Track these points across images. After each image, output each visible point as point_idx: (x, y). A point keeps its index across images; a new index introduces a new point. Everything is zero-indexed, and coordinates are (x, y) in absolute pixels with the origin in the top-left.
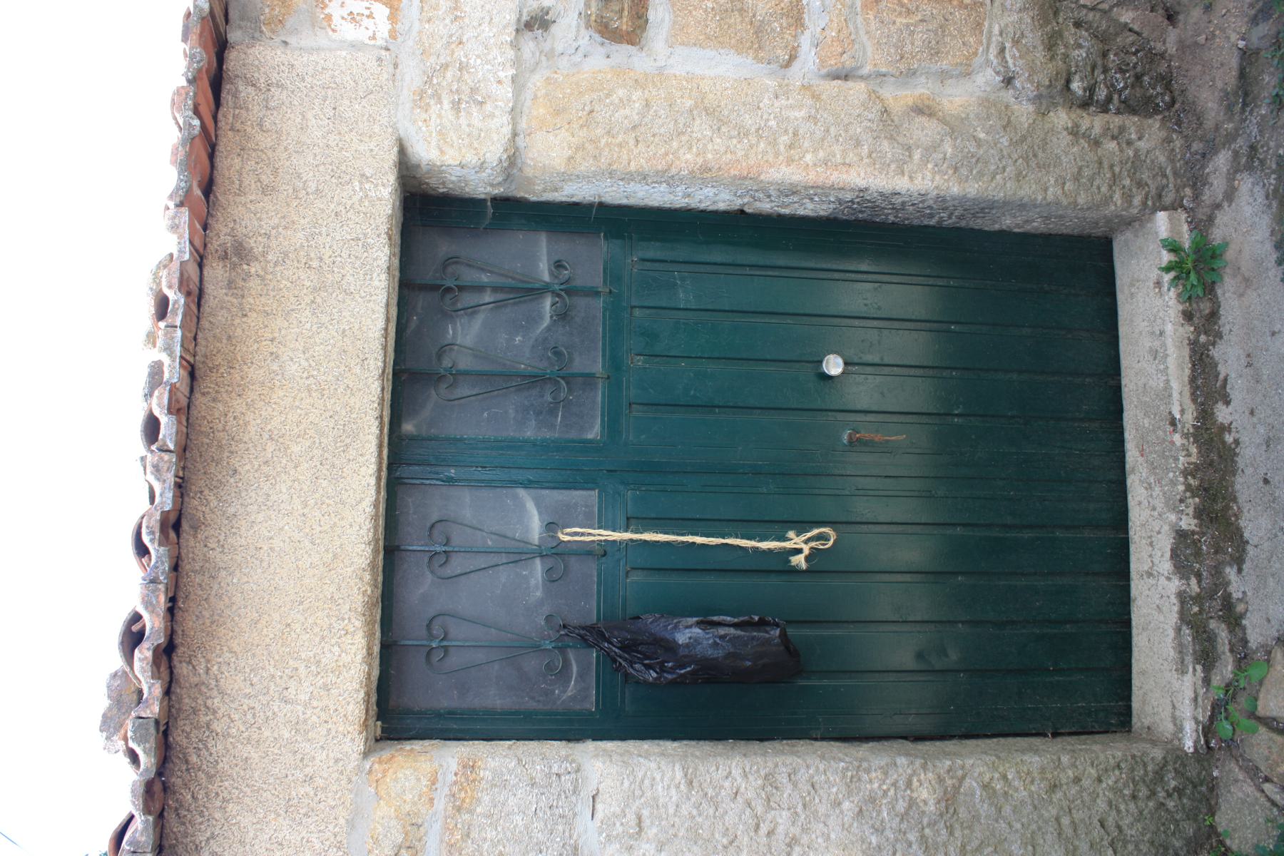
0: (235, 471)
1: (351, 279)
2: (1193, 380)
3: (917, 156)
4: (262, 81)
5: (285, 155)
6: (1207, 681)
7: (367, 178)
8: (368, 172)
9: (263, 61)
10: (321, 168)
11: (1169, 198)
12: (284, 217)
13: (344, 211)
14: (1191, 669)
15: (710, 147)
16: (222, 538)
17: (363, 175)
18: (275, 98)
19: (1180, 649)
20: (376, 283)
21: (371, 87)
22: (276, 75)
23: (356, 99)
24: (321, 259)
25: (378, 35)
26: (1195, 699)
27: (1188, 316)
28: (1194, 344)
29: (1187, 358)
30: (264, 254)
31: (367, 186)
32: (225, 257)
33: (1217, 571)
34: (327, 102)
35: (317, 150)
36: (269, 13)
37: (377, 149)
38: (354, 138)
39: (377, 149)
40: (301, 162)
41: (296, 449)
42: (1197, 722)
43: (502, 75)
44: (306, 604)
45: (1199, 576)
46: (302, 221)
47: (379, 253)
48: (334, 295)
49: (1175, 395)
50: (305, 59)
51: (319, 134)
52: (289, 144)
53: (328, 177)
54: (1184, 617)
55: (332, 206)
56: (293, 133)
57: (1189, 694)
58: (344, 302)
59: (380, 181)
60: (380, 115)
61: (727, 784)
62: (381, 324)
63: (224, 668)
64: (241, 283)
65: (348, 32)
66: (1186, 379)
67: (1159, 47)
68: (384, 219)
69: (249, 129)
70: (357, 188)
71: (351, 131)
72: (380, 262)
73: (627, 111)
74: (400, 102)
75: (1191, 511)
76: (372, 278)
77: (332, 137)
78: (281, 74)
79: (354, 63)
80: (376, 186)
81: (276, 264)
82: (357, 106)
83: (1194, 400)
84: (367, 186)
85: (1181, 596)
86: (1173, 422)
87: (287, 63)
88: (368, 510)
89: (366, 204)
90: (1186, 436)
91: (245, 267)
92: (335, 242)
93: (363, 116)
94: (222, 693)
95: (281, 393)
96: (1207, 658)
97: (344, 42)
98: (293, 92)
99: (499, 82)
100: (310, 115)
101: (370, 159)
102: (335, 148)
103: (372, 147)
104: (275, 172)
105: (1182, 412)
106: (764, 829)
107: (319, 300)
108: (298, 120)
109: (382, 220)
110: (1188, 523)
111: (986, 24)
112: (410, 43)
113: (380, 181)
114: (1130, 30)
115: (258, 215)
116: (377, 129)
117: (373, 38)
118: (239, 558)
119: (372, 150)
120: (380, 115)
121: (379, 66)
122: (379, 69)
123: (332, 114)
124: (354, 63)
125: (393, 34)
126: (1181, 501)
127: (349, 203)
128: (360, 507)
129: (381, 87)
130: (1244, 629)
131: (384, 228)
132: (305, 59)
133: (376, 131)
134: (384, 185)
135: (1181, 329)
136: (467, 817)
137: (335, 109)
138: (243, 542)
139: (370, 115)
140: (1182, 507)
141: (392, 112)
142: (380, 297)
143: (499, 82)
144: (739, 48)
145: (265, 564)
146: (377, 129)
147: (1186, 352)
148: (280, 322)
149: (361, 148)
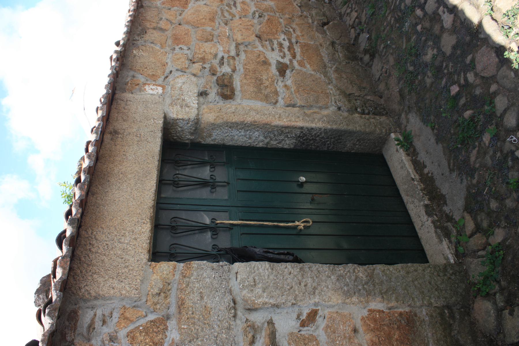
0: (109, 181)
2: (415, 169)
3: (316, 120)
6: (450, 242)
8: (156, 118)
11: (393, 130)
14: (444, 240)
15: (256, 117)
16: (102, 197)
19: (439, 237)
26: (449, 247)
27: (408, 155)
28: (412, 161)
29: (411, 164)
32: (111, 133)
33: (441, 211)
35: (140, 113)
41: (130, 176)
42: (452, 254)
43: (194, 102)
44: (130, 215)
45: (436, 215)
49: (411, 173)
54: (436, 227)
57: (446, 247)
61: (286, 270)
62: (159, 149)
63: (98, 233)
65: (151, 92)
66: (413, 169)
67: (380, 103)
73: (231, 109)
75: (427, 199)
81: (127, 135)
83: (417, 173)
85: (433, 222)
86: (413, 179)
88: (153, 191)
90: (418, 181)
94: (97, 239)
95: (126, 163)
96: (447, 234)
99: (194, 103)
104: (128, 117)
105: (415, 176)
106: (303, 284)
110: (427, 202)
111: (330, 97)
112: (168, 94)
114: (371, 100)
117: (158, 93)
118: (107, 203)
125: (163, 93)
126: (423, 197)
127: (150, 124)
128: (150, 191)
130: (454, 219)
131: (160, 129)
135: (407, 158)
136: (188, 279)
138: (109, 198)
140: (424, 198)
143: (194, 103)
144: (261, 100)
145: (117, 204)
146: (158, 110)
147: (410, 162)
148: (127, 147)
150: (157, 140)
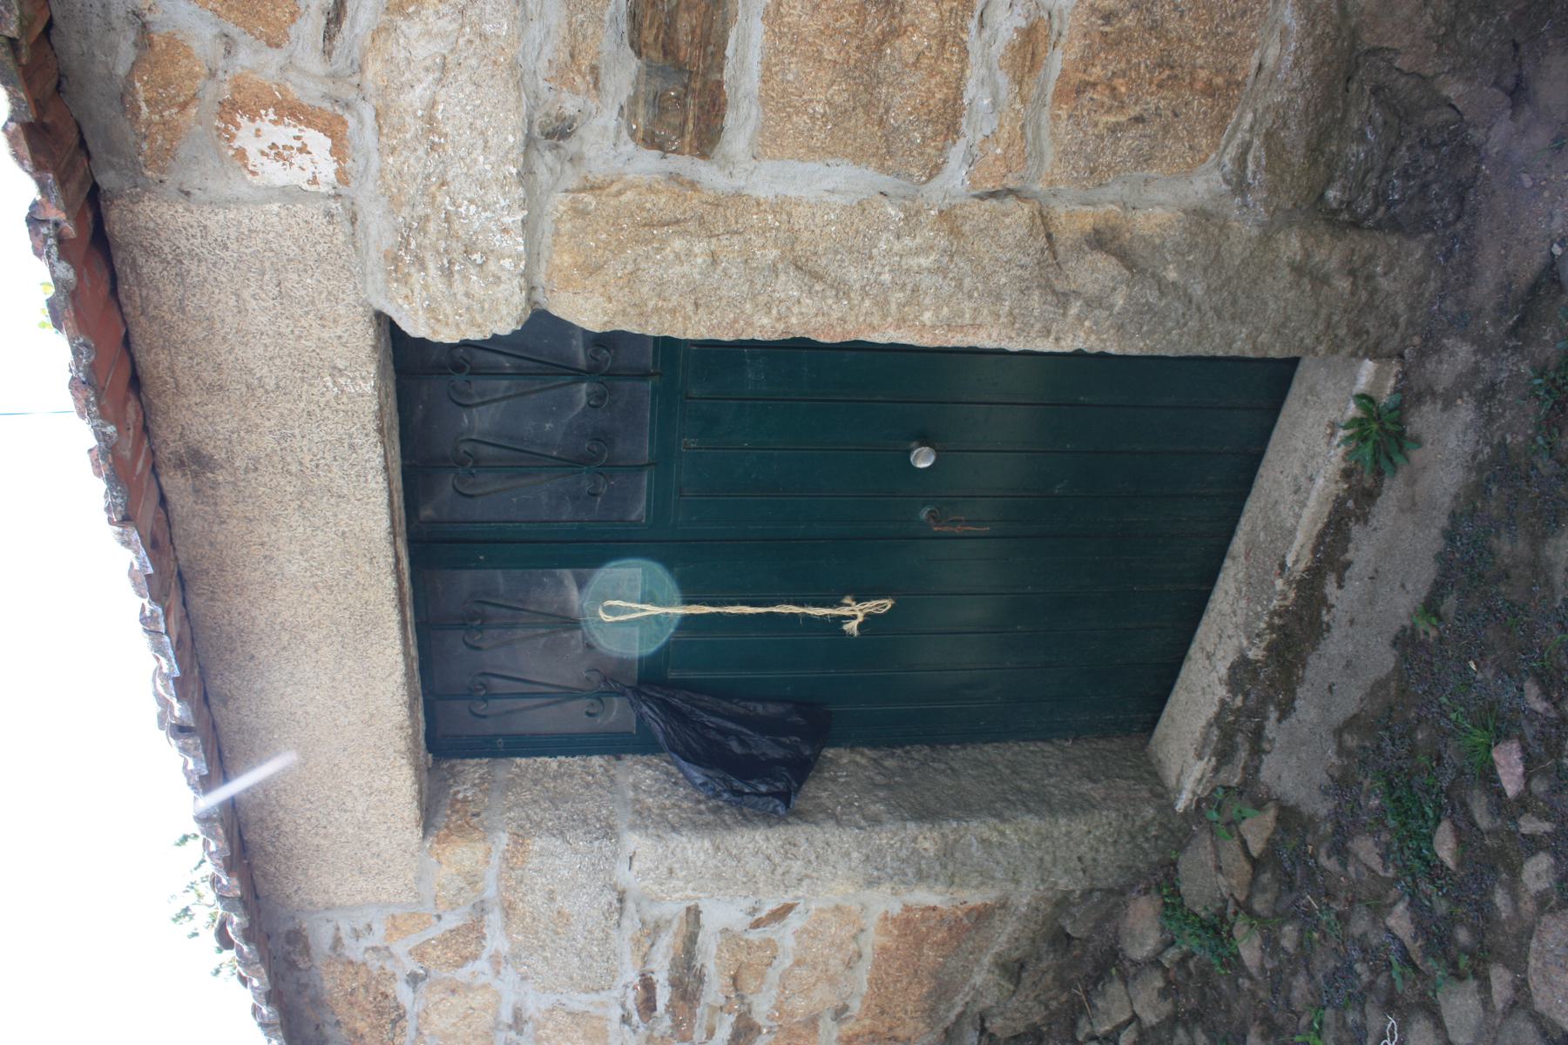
0: (252, 657)
1: (342, 481)
2: (1321, 535)
3: (1074, 310)
4: (167, 250)
5: (226, 347)
6: (1216, 770)
7: (340, 370)
8: (341, 364)
9: (159, 221)
10: (278, 361)
11: (1392, 344)
12: (242, 420)
13: (318, 410)
14: (1206, 759)
15: (796, 310)
16: (254, 708)
17: (335, 368)
18: (192, 273)
19: (1205, 738)
20: (373, 485)
21: (324, 254)
22: (184, 241)
23: (306, 271)
24: (301, 464)
25: (320, 178)
26: (1201, 780)
27: (1347, 474)
28: (1339, 503)
29: (1326, 514)
30: (230, 459)
31: (342, 381)
32: (181, 464)
33: (1263, 702)
34: (267, 277)
36: (150, 148)
37: (346, 335)
39: (346, 335)
40: (250, 355)
41: (312, 637)
42: (1194, 793)
43: (507, 220)
44: (350, 750)
45: (1246, 695)
46: (267, 424)
47: (371, 454)
48: (325, 499)
49: (1296, 545)
50: (221, 217)
51: (265, 319)
52: (227, 333)
54: (1218, 719)
55: (302, 405)
56: (228, 320)
57: (1197, 775)
58: (338, 505)
59: (357, 374)
61: (750, 846)
62: (385, 524)
63: (282, 793)
64: (210, 492)
65: (275, 174)
66: (1315, 533)
67: (1477, 135)
68: (371, 417)
69: (168, 316)
70: (330, 384)
71: (307, 313)
72: (373, 464)
73: (686, 268)
74: (369, 270)
75: (1263, 645)
76: (366, 481)
77: (283, 322)
78: (192, 240)
79: (292, 222)
80: (353, 379)
81: (246, 471)
82: (309, 281)
83: (1315, 550)
84: (342, 381)
85: (1223, 702)
86: (1283, 566)
87: (195, 224)
88: (399, 680)
89: (345, 399)
90: (1288, 583)
91: (210, 475)
92: (313, 445)
93: (321, 293)
94: (282, 807)
95: (285, 591)
96: (1224, 756)
97: (272, 188)
98: (214, 265)
99: (505, 231)
100: (246, 294)
101: (340, 349)
103: (339, 333)
104: (218, 368)
105: (1296, 562)
106: (780, 871)
107: (308, 505)
108: (232, 302)
110: (1255, 654)
111: (1235, 115)
112: (370, 186)
113: (357, 374)
114: (1453, 107)
115: (210, 419)
116: (341, 310)
117: (314, 181)
118: (275, 721)
119: (340, 337)
121: (329, 223)
122: (331, 228)
123: (276, 293)
124: (292, 222)
125: (342, 176)
126: (1258, 635)
127: (323, 401)
128: (390, 679)
130: (1261, 761)
131: (372, 426)
132: (221, 217)
134: (363, 378)
135: (1333, 487)
136: (520, 872)
138: (276, 709)
139: (329, 293)
140: (1256, 641)
141: (359, 286)
142: (380, 499)
143: (505, 231)
144: (859, 156)
145: (303, 724)
146: (341, 310)
147: (1327, 509)
148: (266, 527)
149: (325, 335)
150: (373, 485)
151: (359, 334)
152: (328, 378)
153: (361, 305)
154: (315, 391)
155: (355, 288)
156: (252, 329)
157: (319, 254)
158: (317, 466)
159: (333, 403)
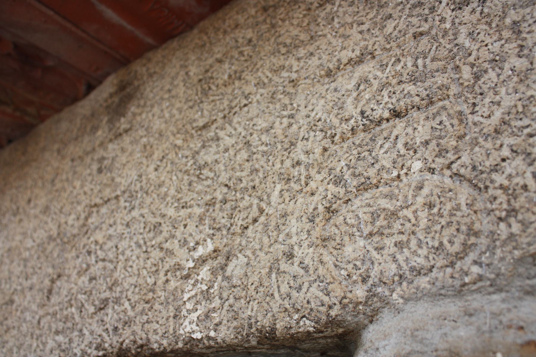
7: (223, 268)
13: (160, 239)
23: (441, 152)
31: (204, 273)
38: (316, 198)
39: (296, 269)
51: (319, 112)
53: (224, 178)
59: (216, 303)
60: (399, 245)
70: (201, 251)
71: (338, 181)
80: (207, 295)
82: (417, 165)
84: (204, 273)
93: (390, 196)
101: (265, 259)
102: (288, 163)
109: (137, 328)
119: (290, 256)
120: (399, 245)
123: (377, 115)
127: (173, 245)
129: (512, 212)
133: (348, 250)
137: (396, 114)
139: (394, 214)
141: (423, 282)
151: (299, 297)
152: (210, 246)
153: (371, 294)
154: (191, 228)
155: (418, 272)
156: (300, 100)
157: (495, 169)
158: (89, 253)
159: (170, 262)
